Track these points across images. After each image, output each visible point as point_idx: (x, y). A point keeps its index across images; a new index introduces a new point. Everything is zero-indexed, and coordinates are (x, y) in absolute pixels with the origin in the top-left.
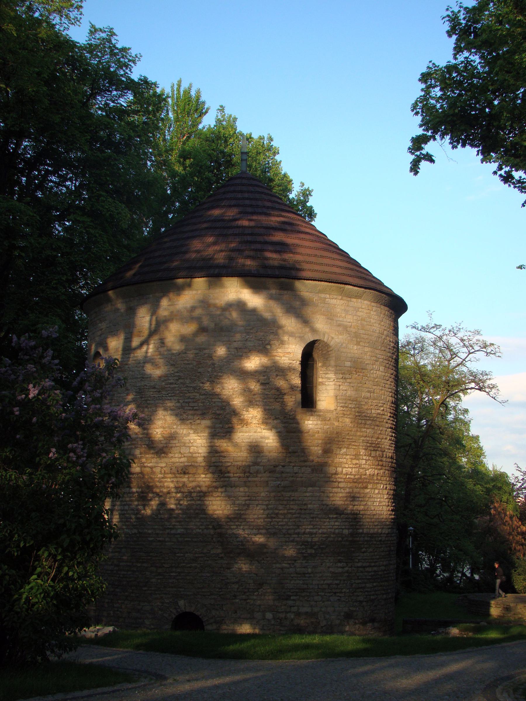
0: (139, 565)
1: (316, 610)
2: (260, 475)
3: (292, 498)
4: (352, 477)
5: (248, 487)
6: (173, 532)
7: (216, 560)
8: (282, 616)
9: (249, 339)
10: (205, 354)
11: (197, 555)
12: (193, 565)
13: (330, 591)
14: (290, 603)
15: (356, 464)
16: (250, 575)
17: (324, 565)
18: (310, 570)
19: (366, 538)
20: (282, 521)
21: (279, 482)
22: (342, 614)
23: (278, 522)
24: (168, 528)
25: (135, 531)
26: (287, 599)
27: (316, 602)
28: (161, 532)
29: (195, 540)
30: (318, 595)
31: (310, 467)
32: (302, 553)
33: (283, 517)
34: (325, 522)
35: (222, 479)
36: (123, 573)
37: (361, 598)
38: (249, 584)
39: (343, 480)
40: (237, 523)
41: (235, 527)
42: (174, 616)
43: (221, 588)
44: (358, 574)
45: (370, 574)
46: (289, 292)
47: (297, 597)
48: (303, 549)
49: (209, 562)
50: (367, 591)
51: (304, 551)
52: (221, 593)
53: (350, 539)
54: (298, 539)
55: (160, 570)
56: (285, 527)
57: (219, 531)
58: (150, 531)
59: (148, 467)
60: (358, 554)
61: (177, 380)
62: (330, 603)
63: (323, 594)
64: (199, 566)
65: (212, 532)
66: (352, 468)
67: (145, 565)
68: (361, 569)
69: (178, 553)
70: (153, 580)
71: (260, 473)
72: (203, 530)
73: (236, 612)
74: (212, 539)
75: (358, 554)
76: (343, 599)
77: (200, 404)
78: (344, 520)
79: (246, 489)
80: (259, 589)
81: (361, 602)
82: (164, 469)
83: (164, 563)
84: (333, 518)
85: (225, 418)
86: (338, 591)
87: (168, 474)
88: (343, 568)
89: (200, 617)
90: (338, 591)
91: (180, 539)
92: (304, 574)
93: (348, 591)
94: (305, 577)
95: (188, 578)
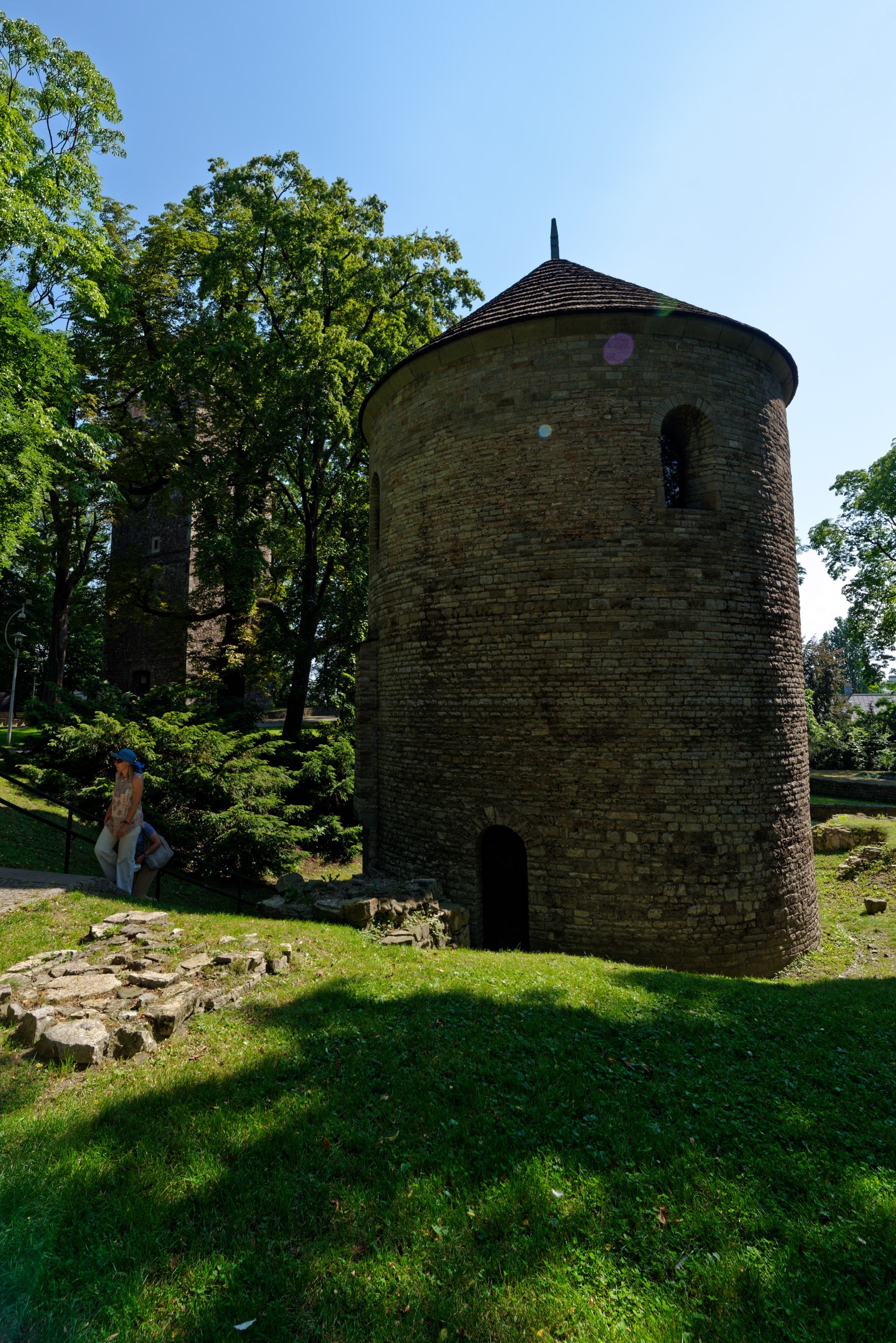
0: (427, 751)
1: (709, 828)
2: (604, 613)
4: (752, 616)
5: (588, 631)
6: (474, 703)
8: (654, 838)
13: (729, 797)
14: (666, 817)
15: (756, 597)
17: (717, 753)
22: (751, 834)
25: (421, 702)
28: (456, 703)
29: (506, 715)
30: (711, 805)
31: (685, 598)
34: (713, 687)
36: (407, 761)
39: (738, 621)
40: (571, 689)
41: (569, 694)
42: (479, 831)
43: (550, 791)
44: (770, 770)
53: (756, 713)
54: (673, 714)
55: (456, 761)
56: (650, 694)
57: (544, 701)
58: (440, 703)
60: (767, 738)
61: (472, 480)
65: (532, 702)
66: (750, 602)
67: (435, 751)
71: (606, 609)
72: (518, 698)
73: (577, 830)
75: (767, 738)
76: (750, 810)
77: (506, 511)
78: (743, 684)
79: (584, 636)
80: (611, 793)
84: (726, 680)
86: (741, 797)
90: (741, 797)
92: (686, 769)
94: (688, 774)
95: (498, 772)
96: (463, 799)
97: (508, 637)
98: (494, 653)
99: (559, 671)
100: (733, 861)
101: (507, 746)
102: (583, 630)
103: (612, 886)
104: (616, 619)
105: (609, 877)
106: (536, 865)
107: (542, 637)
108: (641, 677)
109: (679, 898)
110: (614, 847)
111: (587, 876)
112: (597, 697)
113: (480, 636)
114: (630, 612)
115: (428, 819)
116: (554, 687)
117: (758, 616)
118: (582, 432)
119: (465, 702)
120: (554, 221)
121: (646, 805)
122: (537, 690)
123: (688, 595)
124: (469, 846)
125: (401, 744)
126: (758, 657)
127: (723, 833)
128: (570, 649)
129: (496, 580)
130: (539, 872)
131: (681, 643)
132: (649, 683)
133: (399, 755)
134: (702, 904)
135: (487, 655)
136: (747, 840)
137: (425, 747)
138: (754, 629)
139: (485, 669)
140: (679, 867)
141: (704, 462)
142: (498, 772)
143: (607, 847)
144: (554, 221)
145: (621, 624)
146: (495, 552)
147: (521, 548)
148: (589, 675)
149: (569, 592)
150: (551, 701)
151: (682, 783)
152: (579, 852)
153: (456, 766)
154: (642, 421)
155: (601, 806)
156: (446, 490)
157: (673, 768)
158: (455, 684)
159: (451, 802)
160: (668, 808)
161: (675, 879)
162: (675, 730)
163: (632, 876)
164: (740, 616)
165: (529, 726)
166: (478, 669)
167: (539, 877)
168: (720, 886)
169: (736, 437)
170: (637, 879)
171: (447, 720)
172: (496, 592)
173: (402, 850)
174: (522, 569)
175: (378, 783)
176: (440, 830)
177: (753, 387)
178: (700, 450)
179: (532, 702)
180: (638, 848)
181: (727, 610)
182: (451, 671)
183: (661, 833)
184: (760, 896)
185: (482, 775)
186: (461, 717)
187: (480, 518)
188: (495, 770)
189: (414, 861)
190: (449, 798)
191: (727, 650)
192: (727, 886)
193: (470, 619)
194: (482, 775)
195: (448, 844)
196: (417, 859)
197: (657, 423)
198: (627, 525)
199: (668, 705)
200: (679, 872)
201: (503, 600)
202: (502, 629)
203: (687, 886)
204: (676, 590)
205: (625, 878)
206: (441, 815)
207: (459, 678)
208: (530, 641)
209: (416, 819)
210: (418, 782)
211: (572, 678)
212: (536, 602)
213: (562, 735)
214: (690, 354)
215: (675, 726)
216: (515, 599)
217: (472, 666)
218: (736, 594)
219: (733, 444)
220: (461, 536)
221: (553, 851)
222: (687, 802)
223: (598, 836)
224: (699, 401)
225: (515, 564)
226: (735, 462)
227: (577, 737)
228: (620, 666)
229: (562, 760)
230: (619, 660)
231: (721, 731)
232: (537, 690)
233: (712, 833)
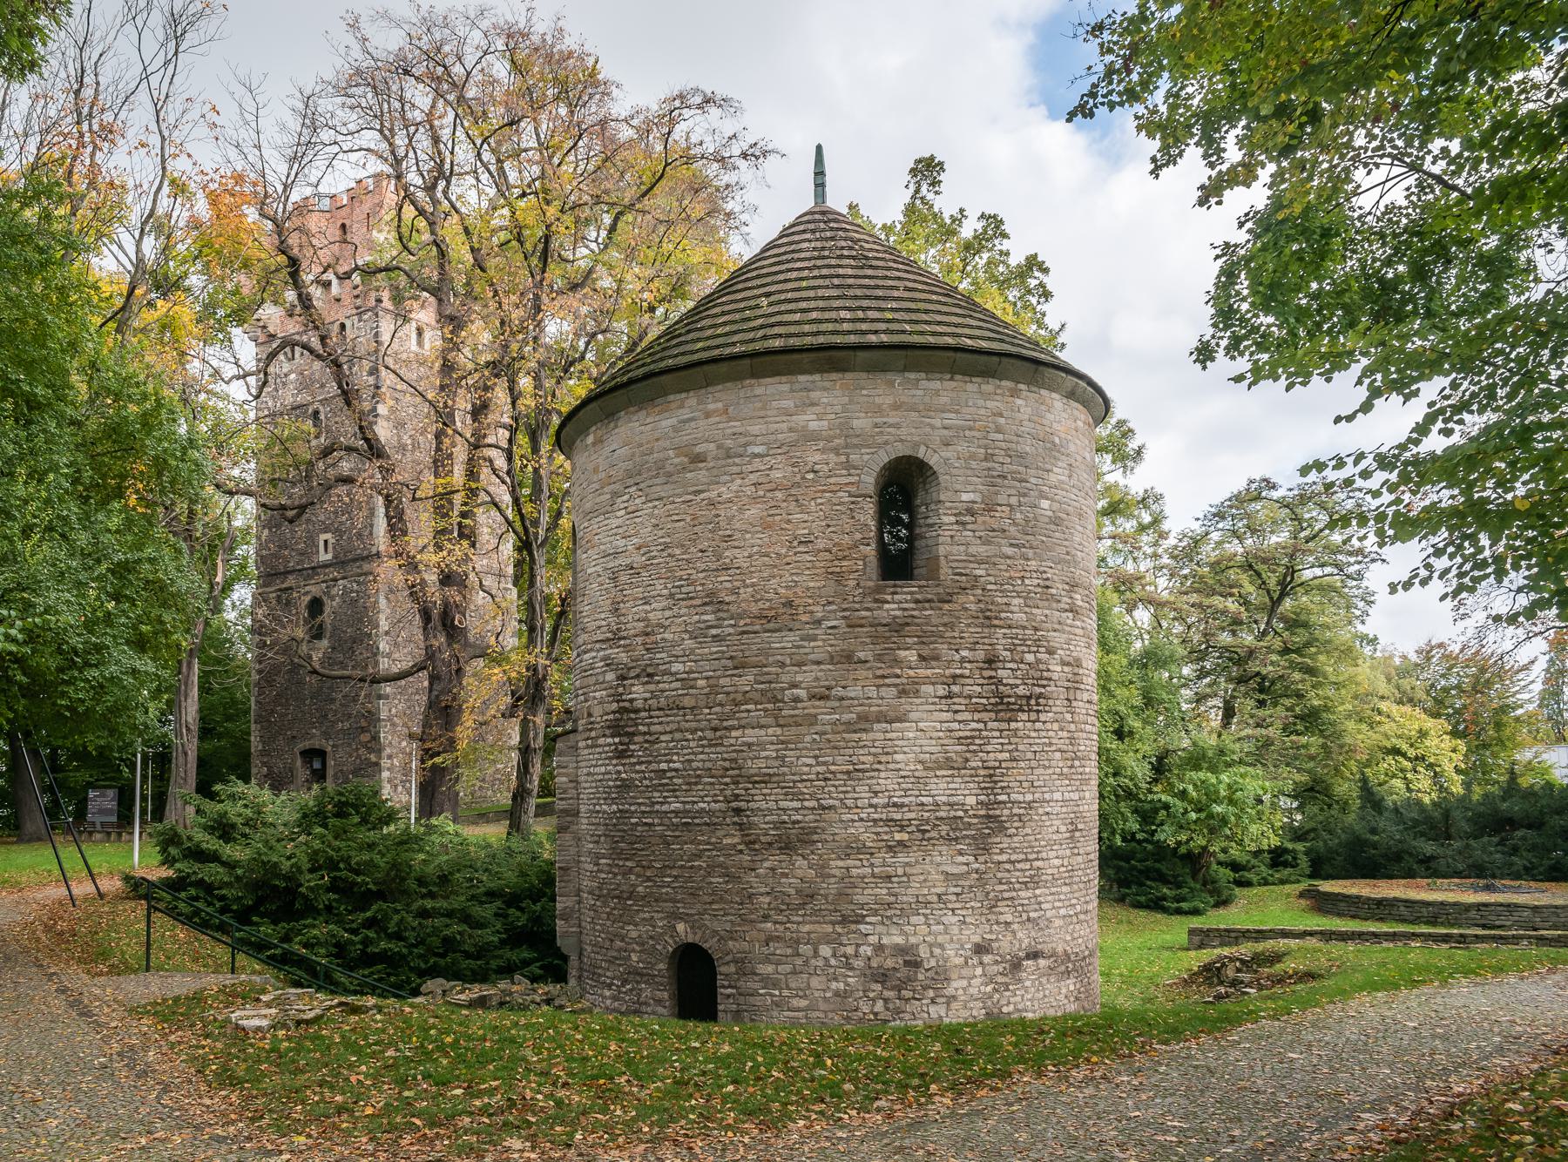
1: (913, 940)
4: (984, 701)
8: (850, 950)
17: (928, 859)
18: (900, 871)
19: (1016, 811)
34: (926, 784)
37: (1009, 918)
44: (999, 875)
53: (983, 812)
57: (733, 804)
65: (722, 806)
67: (629, 864)
68: (1007, 866)
70: (640, 889)
76: (968, 920)
79: (779, 731)
86: (958, 905)
90: (958, 905)
99: (752, 771)
100: (941, 976)
101: (698, 856)
102: (779, 726)
103: (803, 1003)
104: (813, 711)
107: (734, 734)
109: (876, 1014)
110: (806, 963)
114: (830, 704)
115: (622, 940)
117: (993, 701)
118: (779, 495)
122: (728, 793)
123: (898, 681)
124: (661, 966)
125: (598, 856)
126: (989, 748)
127: (931, 946)
128: (762, 746)
130: (729, 991)
131: (889, 736)
138: (985, 716)
139: (676, 770)
141: (930, 521)
143: (799, 961)
147: (714, 632)
148: (784, 774)
150: (742, 804)
151: (884, 891)
152: (770, 969)
153: (649, 879)
154: (852, 479)
155: (795, 919)
156: (638, 560)
157: (873, 876)
162: (877, 834)
165: (720, 833)
166: (671, 770)
167: (729, 996)
169: (970, 488)
170: (828, 995)
172: (687, 682)
176: (634, 951)
177: (1002, 421)
178: (927, 505)
179: (722, 806)
180: (833, 962)
181: (949, 696)
183: (858, 945)
184: (975, 1013)
187: (672, 595)
189: (609, 986)
190: (642, 915)
191: (945, 742)
192: (933, 1002)
197: (869, 481)
198: (830, 603)
199: (871, 806)
200: (878, 987)
202: (694, 725)
203: (886, 1001)
204: (884, 677)
205: (817, 994)
206: (634, 934)
207: (651, 779)
211: (766, 780)
212: (728, 693)
213: (754, 843)
214: (914, 392)
217: (664, 766)
218: (962, 676)
219: (965, 497)
220: (651, 616)
221: (744, 967)
222: (889, 913)
223: (789, 951)
224: (923, 449)
226: (968, 518)
227: (770, 844)
228: (818, 764)
230: (816, 757)
231: (934, 834)
232: (728, 793)
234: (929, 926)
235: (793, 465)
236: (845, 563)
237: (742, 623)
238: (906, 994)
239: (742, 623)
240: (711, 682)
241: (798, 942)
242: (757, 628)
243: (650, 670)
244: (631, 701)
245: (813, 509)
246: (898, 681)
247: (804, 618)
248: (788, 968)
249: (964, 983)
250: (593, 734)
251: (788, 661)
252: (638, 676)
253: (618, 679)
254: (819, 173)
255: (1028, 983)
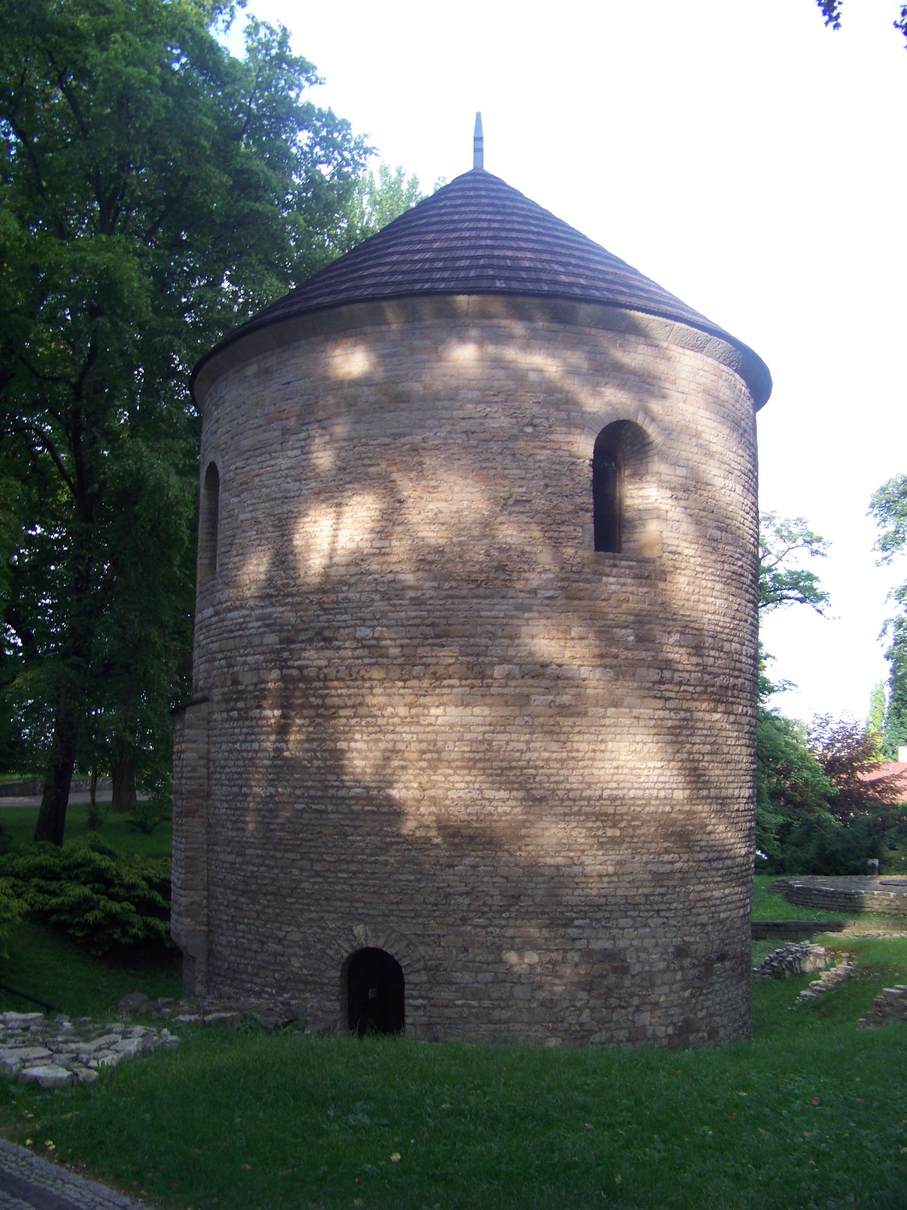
0: (279, 855)
1: (621, 944)
2: (512, 683)
3: (576, 729)
6: (342, 793)
7: (426, 850)
9: (491, 415)
10: (404, 444)
11: (388, 840)
12: (381, 858)
13: (648, 907)
14: (571, 931)
16: (495, 880)
20: (558, 775)
21: (551, 698)
22: (671, 950)
23: (549, 776)
24: (332, 787)
26: (565, 926)
27: (623, 929)
30: (627, 917)
32: (595, 836)
33: (559, 766)
34: (639, 776)
35: (438, 691)
36: (251, 868)
37: (704, 919)
38: (492, 896)
39: (673, 695)
42: (346, 955)
43: (436, 905)
44: (699, 874)
45: (720, 873)
46: (569, 327)
47: (587, 921)
48: (598, 828)
49: (413, 853)
50: (715, 906)
51: (600, 833)
52: (437, 913)
53: (687, 808)
54: (588, 809)
55: (318, 867)
58: (298, 792)
59: (293, 667)
62: (648, 930)
63: (636, 913)
64: (392, 860)
67: (289, 855)
68: (705, 865)
69: (352, 835)
71: (514, 678)
73: (466, 950)
74: (418, 808)
76: (672, 922)
80: (511, 905)
81: (704, 925)
82: (325, 671)
83: (327, 854)
85: (443, 569)
86: (663, 907)
87: (331, 680)
88: (672, 863)
89: (396, 958)
90: (663, 907)
91: (355, 808)
93: (681, 906)
95: (371, 882)
96: (326, 915)
97: (390, 709)
98: (371, 729)
104: (526, 690)
105: (502, 1004)
106: (415, 993)
107: (433, 711)
108: (554, 765)
109: (581, 1025)
111: (475, 1003)
112: (498, 790)
113: (353, 706)
116: (446, 776)
117: (699, 689)
119: (331, 792)
120: (478, 115)
121: (550, 919)
129: (377, 635)
130: (420, 1001)
132: (561, 772)
133: (239, 859)
134: (607, 1030)
135: (362, 732)
136: (665, 956)
137: (277, 850)
140: (584, 990)
142: (371, 882)
144: (478, 115)
145: (532, 697)
146: (377, 597)
149: (471, 655)
152: (467, 977)
153: (317, 874)
155: (496, 922)
158: (319, 768)
159: (310, 919)
160: (576, 923)
161: (579, 1004)
162: (590, 829)
163: (529, 1001)
164: (677, 689)
167: (418, 1007)
168: (630, 1010)
170: (534, 1005)
171: (306, 816)
173: (243, 981)
174: (411, 622)
175: (208, 898)
176: (295, 955)
179: (417, 794)
182: (314, 751)
183: (566, 951)
184: (675, 1020)
185: (351, 885)
186: (325, 811)
188: (367, 879)
190: (307, 915)
193: (342, 684)
194: (351, 885)
195: (305, 972)
196: (263, 992)
200: (584, 995)
201: (385, 661)
203: (592, 1010)
205: (521, 1004)
206: (296, 937)
207: (324, 760)
208: (417, 716)
209: (263, 943)
210: (265, 894)
212: (427, 665)
215: (590, 825)
216: (400, 661)
222: (600, 915)
225: (403, 614)
229: (451, 866)
233: (626, 949)
234: (636, 929)
235: (510, 416)
236: (563, 528)
237: (447, 585)
238: (613, 1002)
239: (447, 585)
240: (407, 651)
241: (500, 948)
242: (464, 592)
243: (326, 633)
244: (300, 668)
245: (531, 465)
246: (614, 662)
247: (518, 586)
248: (489, 977)
249: (666, 989)
250: (241, 704)
251: (499, 633)
252: (310, 640)
253: (282, 642)
254: (478, 139)
255: (717, 986)
